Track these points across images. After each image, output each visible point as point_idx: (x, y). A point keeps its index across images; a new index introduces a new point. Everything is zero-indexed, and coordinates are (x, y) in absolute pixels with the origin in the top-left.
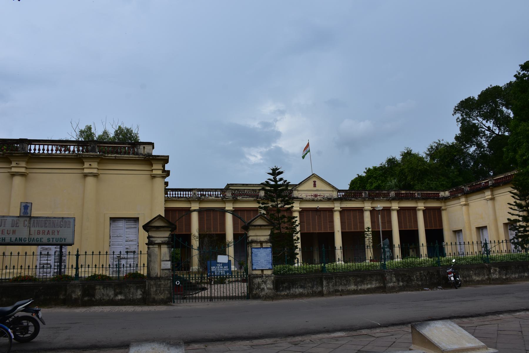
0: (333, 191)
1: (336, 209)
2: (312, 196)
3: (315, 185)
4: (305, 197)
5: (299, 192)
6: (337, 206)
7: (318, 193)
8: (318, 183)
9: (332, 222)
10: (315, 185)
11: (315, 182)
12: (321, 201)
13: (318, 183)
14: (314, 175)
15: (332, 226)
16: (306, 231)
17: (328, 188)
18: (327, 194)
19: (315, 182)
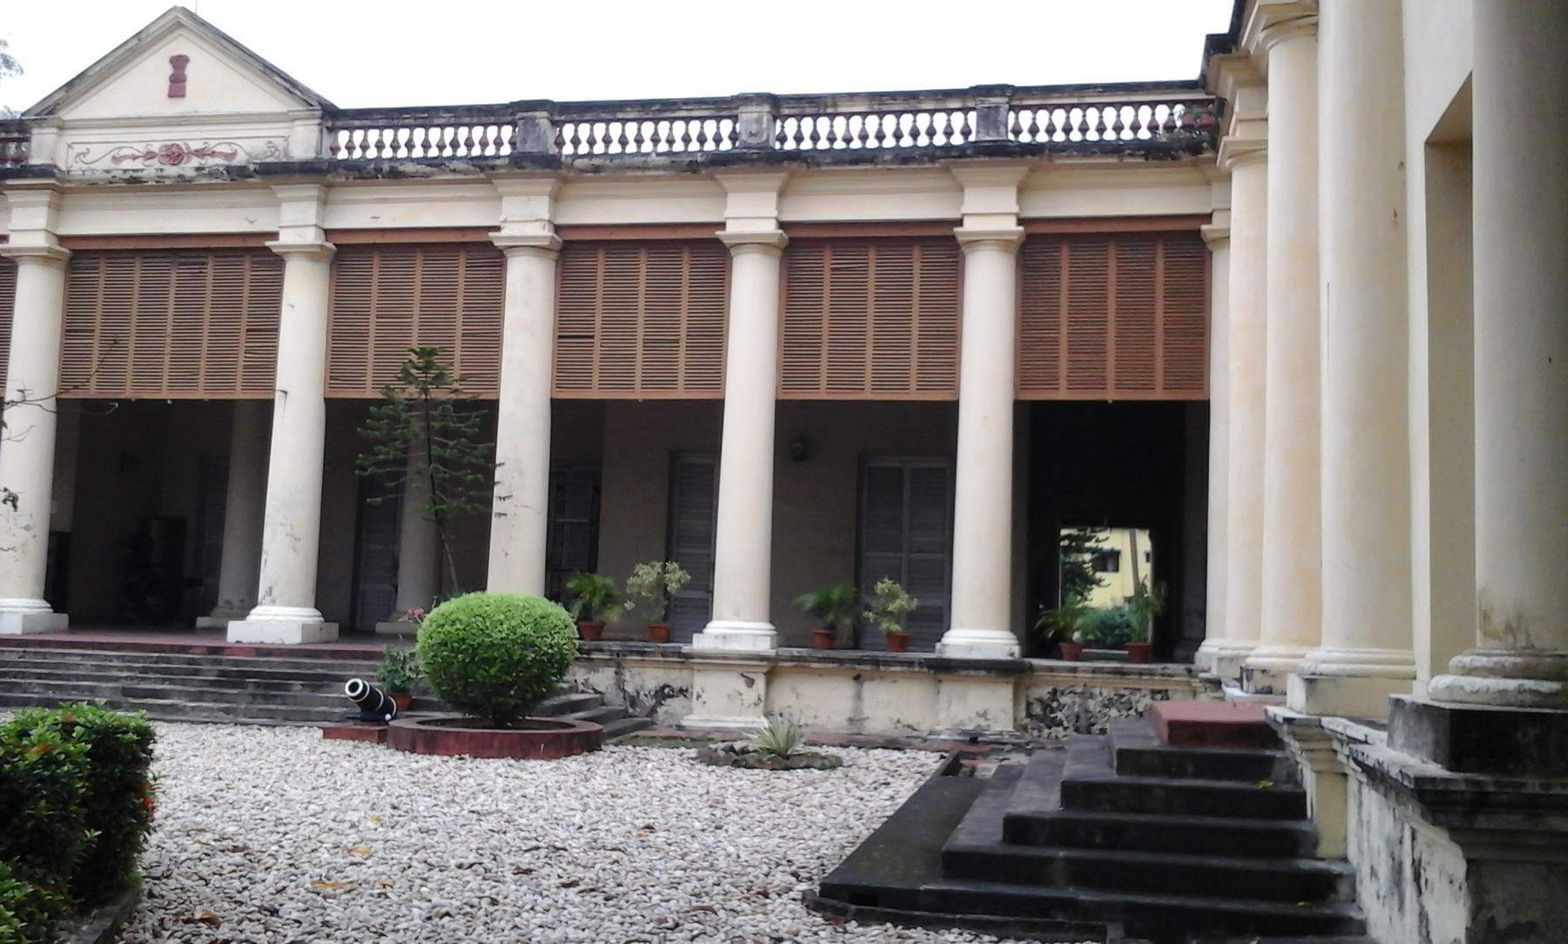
0: (288, 118)
1: (286, 238)
2: (150, 155)
3: (177, 87)
4: (107, 163)
5: (71, 137)
6: (295, 222)
7: (192, 138)
8: (205, 69)
9: (267, 330)
10: (177, 87)
11: (179, 62)
12: (183, 185)
13: (205, 69)
14: (182, 22)
15: (265, 365)
16: (92, 391)
17: (267, 100)
18: (249, 146)
19: (179, 62)
